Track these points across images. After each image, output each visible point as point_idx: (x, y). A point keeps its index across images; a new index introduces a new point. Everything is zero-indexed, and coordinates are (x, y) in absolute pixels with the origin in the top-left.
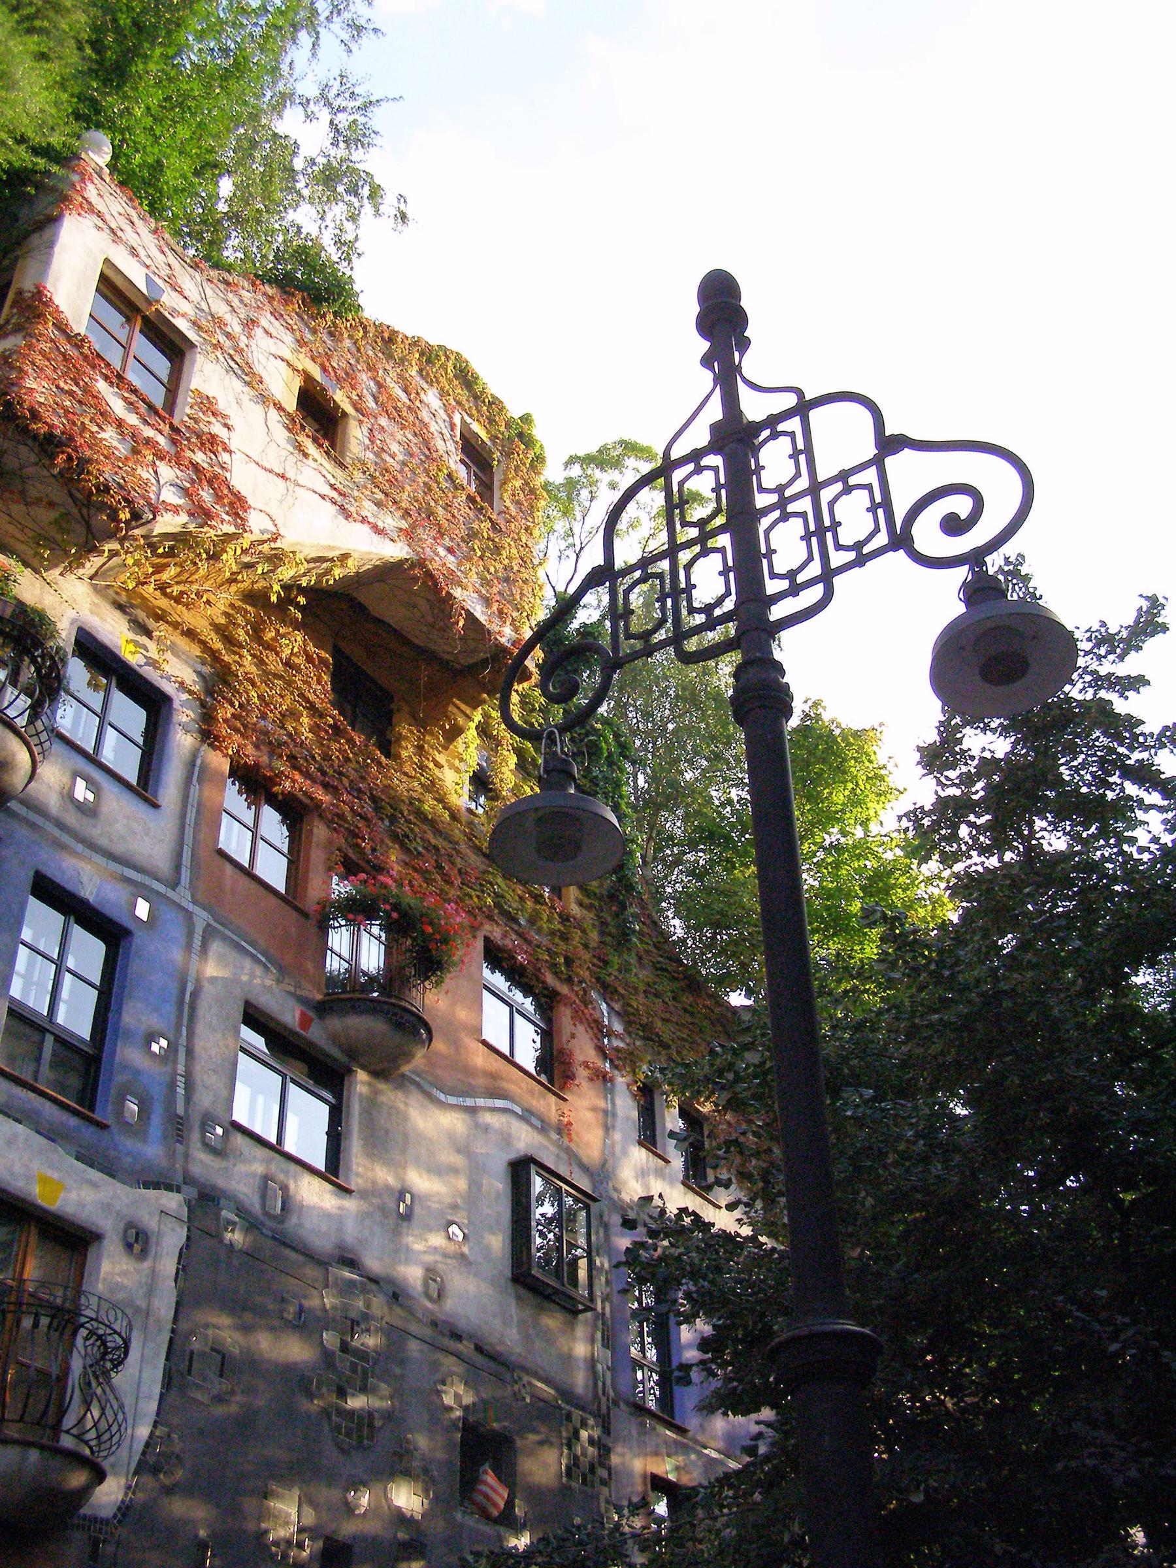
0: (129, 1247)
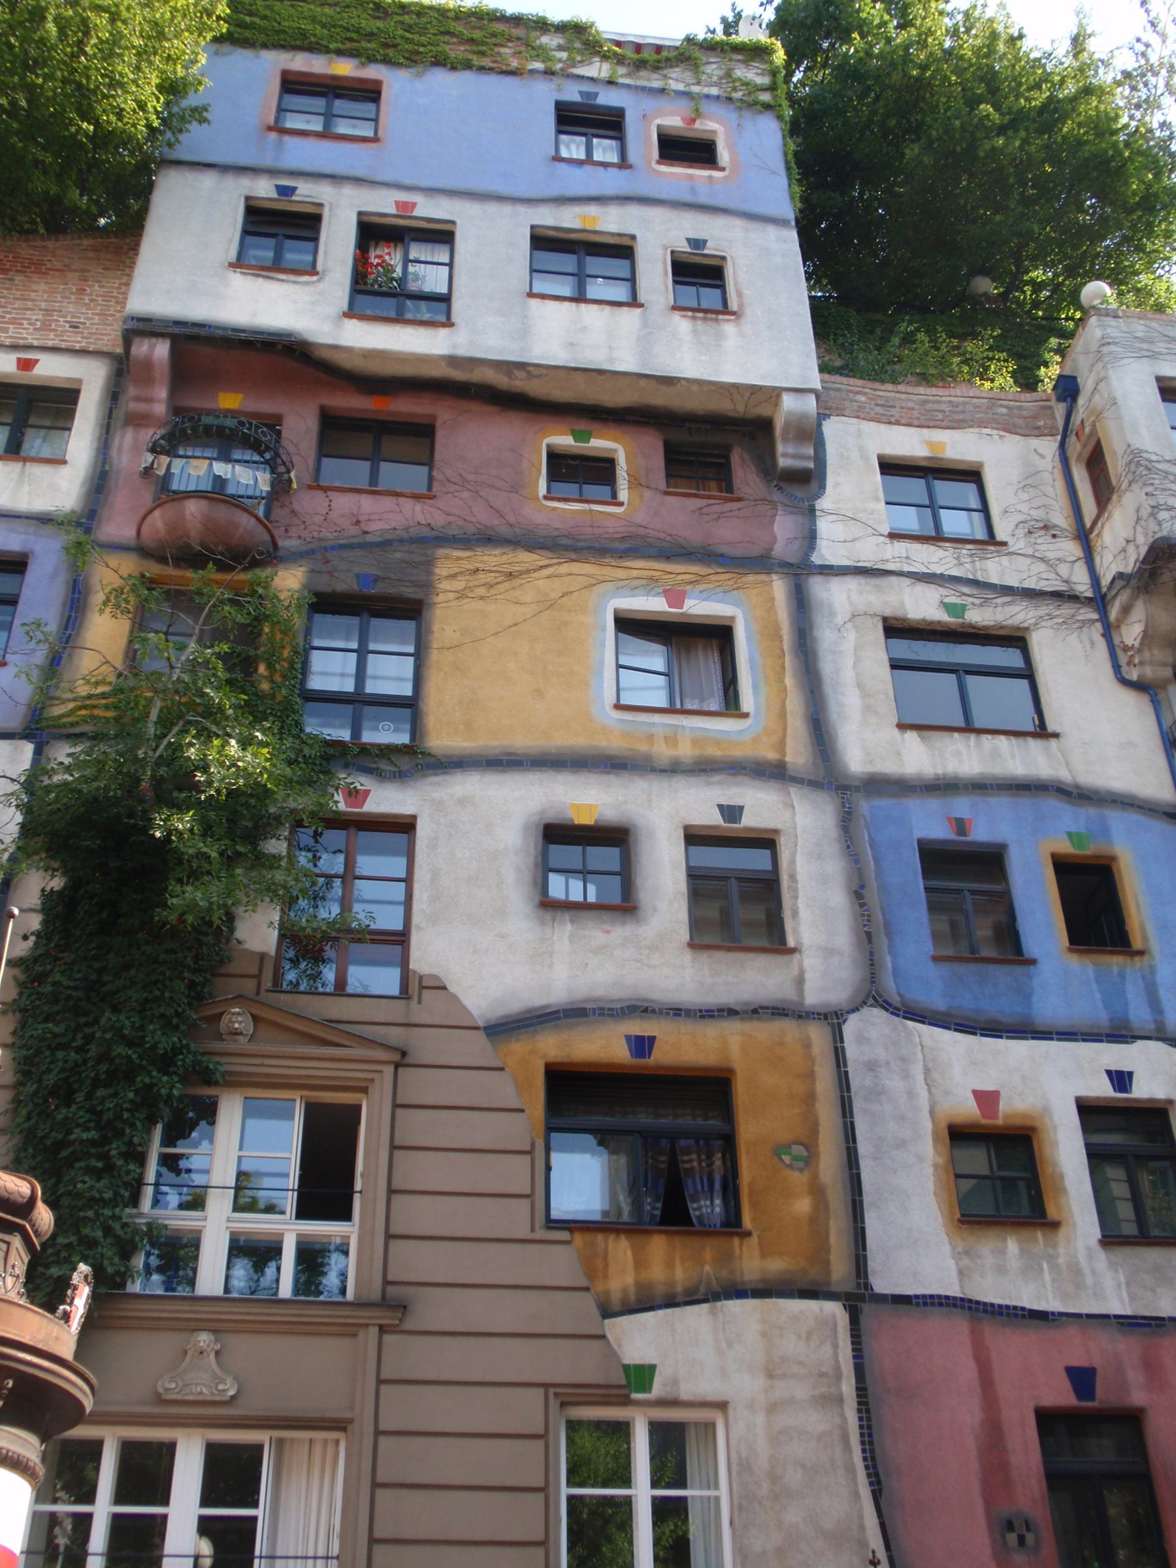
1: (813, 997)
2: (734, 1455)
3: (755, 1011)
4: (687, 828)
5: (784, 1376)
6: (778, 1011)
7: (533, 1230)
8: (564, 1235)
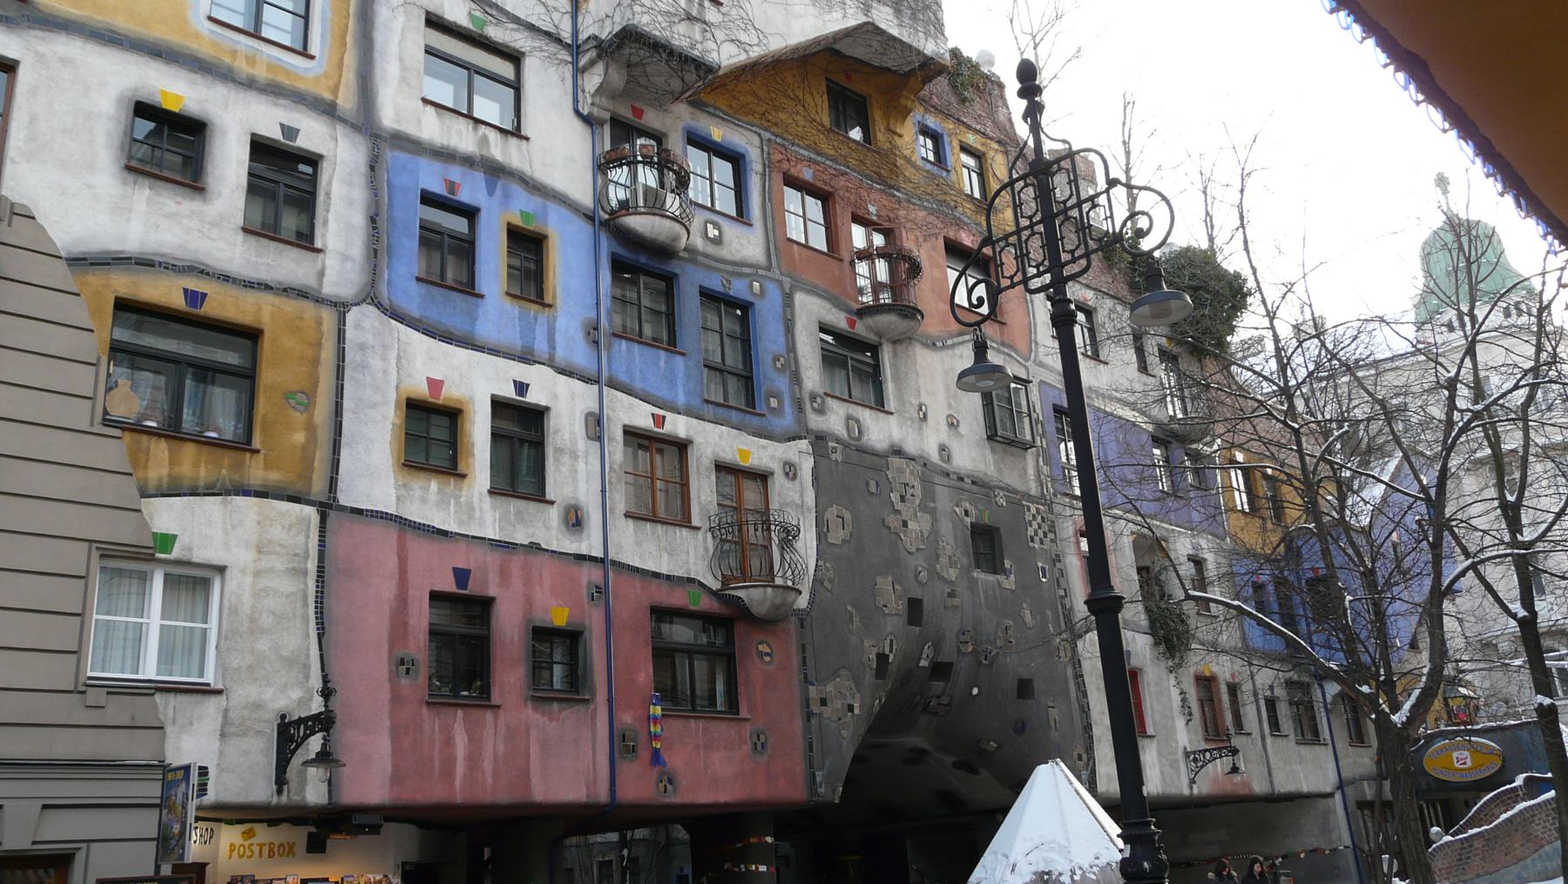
0: (787, 474)
1: (328, 289)
2: (226, 602)
3: (285, 290)
4: (253, 135)
5: (269, 553)
6: (302, 294)
7: (92, 425)
8: (117, 433)
